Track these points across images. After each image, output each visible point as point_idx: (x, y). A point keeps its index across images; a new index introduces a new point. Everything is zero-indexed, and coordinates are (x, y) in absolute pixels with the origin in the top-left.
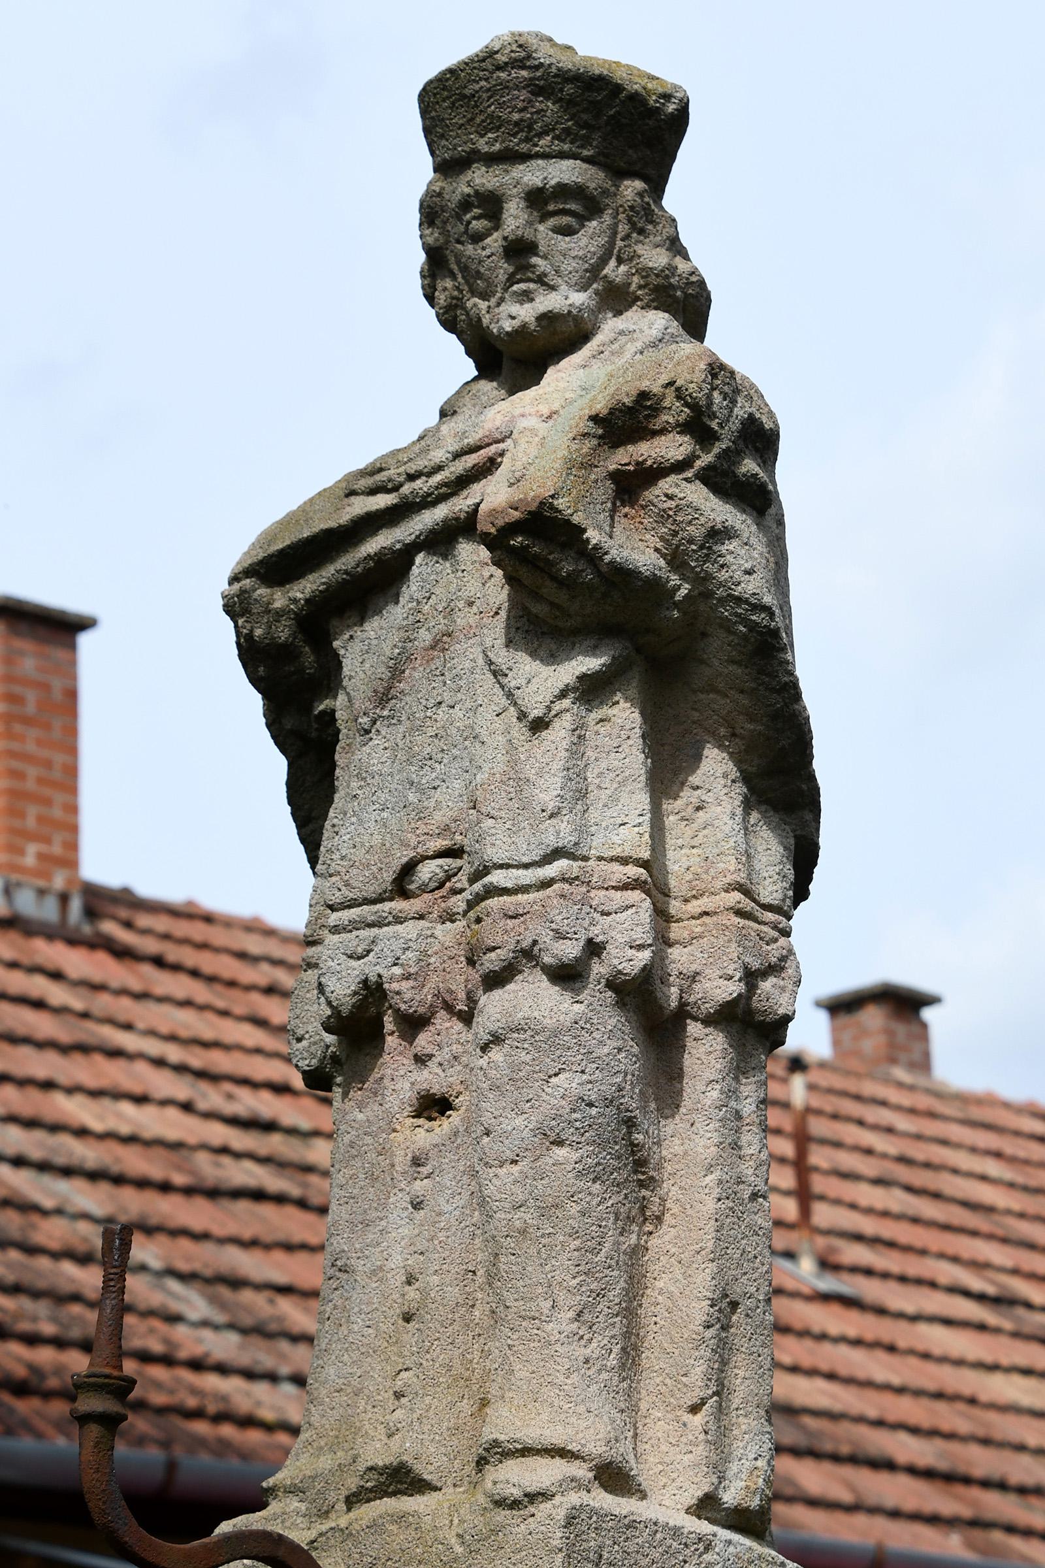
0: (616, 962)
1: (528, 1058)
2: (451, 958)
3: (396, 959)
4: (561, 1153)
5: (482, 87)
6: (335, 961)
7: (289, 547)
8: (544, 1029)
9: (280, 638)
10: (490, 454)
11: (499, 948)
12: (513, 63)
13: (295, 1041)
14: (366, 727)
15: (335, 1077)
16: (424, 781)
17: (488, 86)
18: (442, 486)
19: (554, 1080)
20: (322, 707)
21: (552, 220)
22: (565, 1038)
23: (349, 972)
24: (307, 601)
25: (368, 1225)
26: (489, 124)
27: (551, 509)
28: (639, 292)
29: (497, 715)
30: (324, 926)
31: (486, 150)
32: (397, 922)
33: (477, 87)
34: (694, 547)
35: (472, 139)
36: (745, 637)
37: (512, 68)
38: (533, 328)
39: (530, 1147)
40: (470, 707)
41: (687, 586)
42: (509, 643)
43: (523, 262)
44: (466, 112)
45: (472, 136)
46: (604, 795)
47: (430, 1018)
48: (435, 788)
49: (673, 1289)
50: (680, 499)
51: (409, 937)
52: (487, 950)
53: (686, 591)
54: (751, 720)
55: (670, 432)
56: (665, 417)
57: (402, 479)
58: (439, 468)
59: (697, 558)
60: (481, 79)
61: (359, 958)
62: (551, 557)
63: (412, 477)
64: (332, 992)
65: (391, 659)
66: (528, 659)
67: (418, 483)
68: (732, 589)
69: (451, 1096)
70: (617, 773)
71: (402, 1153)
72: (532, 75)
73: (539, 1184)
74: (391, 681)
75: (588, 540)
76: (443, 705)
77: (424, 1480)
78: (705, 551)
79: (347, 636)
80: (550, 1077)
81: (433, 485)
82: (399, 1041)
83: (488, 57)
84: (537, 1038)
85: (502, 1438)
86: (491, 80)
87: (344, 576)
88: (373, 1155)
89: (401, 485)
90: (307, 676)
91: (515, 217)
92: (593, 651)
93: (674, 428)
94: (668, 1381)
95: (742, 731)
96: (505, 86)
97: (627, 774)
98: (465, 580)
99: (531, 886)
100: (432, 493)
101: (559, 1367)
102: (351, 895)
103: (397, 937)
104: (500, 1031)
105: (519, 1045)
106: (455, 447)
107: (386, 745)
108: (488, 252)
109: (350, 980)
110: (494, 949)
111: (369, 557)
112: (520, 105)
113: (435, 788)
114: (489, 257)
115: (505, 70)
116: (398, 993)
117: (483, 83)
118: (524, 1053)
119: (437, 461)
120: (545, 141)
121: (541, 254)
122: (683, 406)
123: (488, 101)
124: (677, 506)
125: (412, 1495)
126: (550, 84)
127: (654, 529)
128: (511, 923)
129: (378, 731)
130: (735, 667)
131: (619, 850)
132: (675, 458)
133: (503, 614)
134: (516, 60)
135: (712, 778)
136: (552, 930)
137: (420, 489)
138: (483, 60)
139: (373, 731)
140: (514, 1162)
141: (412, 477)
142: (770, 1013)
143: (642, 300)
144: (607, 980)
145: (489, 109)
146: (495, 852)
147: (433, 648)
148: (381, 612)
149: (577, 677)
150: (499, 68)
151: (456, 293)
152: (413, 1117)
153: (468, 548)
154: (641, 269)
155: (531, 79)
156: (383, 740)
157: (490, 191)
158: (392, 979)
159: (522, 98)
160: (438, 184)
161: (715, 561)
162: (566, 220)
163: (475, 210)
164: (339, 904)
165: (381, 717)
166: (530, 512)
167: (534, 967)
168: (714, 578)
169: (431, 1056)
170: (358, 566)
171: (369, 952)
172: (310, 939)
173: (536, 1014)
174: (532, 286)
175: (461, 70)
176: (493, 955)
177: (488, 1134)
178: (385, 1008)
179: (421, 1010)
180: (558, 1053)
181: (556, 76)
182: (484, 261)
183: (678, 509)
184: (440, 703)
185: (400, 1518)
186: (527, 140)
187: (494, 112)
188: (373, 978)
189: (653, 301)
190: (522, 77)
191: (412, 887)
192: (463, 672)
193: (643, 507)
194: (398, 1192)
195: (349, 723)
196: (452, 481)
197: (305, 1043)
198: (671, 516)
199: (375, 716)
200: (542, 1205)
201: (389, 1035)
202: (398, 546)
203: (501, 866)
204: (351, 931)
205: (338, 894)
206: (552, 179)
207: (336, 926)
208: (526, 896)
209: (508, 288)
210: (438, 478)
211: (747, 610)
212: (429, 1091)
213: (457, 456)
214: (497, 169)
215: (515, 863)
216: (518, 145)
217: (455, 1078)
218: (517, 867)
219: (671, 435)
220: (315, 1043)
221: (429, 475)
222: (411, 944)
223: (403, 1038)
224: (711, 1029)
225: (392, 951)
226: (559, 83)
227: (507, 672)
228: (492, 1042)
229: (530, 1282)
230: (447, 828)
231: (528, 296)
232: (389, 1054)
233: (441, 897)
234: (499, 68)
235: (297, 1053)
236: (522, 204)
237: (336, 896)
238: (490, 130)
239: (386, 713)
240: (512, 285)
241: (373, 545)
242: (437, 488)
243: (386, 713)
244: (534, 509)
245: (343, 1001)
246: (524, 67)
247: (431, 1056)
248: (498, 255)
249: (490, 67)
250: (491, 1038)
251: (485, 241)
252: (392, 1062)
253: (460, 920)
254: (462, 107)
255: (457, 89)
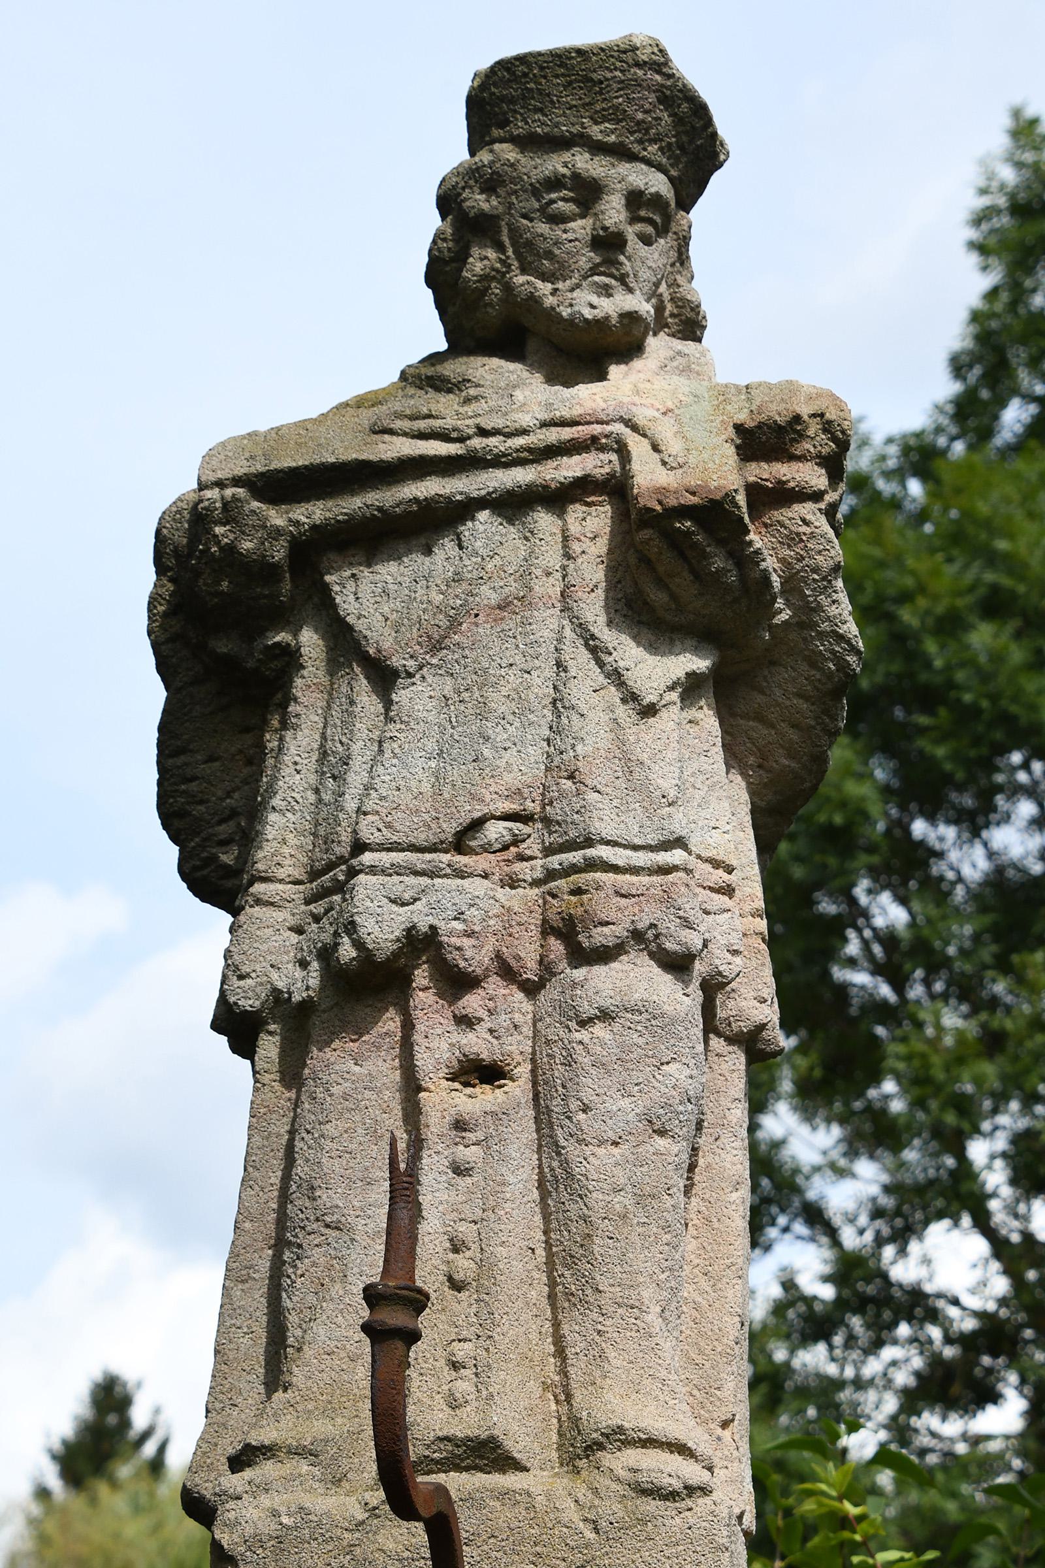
0: (717, 962)
1: (641, 1041)
2: (519, 924)
3: (459, 914)
4: (661, 1143)
5: (615, 77)
6: (375, 902)
7: (306, 467)
8: (663, 1015)
9: (273, 558)
10: (595, 433)
11: (613, 924)
12: (651, 64)
13: (235, 978)
14: (411, 670)
15: (268, 1024)
16: (498, 740)
17: (623, 78)
18: (525, 450)
19: (664, 1067)
20: (278, 639)
21: (639, 225)
22: (679, 1028)
23: (392, 916)
24: (314, 527)
25: (369, 1183)
26: (610, 114)
27: (732, 503)
28: (669, 320)
29: (594, 691)
30: (279, 864)
31: (600, 138)
32: (458, 876)
33: (609, 75)
34: (816, 577)
35: (584, 123)
36: (830, 675)
37: (650, 69)
38: (614, 323)
39: (634, 1131)
41: (788, 612)
42: (610, 623)
43: (612, 257)
44: (585, 95)
45: (584, 120)
46: (698, 795)
47: (481, 981)
48: (505, 749)
49: (700, 1300)
50: (816, 527)
51: (477, 893)
52: (599, 923)
53: (787, 617)
54: (791, 755)
55: (807, 460)
56: (807, 446)
57: (471, 431)
58: (524, 432)
59: (815, 588)
60: (616, 69)
61: (403, 905)
62: (708, 549)
63: (483, 432)
64: (369, 934)
65: (453, 608)
66: (633, 644)
67: (493, 441)
68: (837, 626)
69: (508, 1065)
70: (707, 776)
71: (439, 1115)
72: (664, 82)
73: (638, 1171)
74: (448, 630)
75: (751, 543)
76: (514, 667)
77: (513, 1458)
78: (825, 583)
79: (348, 573)
80: (662, 1064)
81: (513, 447)
82: (436, 998)
83: (630, 51)
84: (653, 1022)
85: (626, 1425)
86: (627, 73)
87: (376, 513)
88: (377, 1112)
89: (469, 438)
90: (277, 603)
91: (613, 211)
92: (696, 651)
93: (812, 458)
94: (695, 1392)
95: (774, 765)
96: (638, 84)
97: (715, 780)
98: (543, 549)
99: (643, 869)
100: (509, 455)
101: (660, 1362)
102: (395, 838)
103: (460, 892)
104: (612, 1008)
105: (632, 1026)
106: (545, 416)
107: (432, 693)
108: (570, 236)
109: (394, 925)
110: (607, 923)
111: (416, 500)
112: (647, 106)
113: (505, 749)
114: (570, 241)
115: (642, 69)
116: (459, 949)
117: (618, 73)
118: (635, 1036)
119: (525, 425)
120: (652, 148)
121: (627, 254)
122: (828, 439)
123: (617, 92)
124: (812, 533)
125: (489, 1473)
126: (673, 97)
127: (774, 549)
128: (624, 902)
129: (423, 677)
130: (801, 701)
131: (714, 852)
132: (819, 487)
133: (600, 593)
134: (655, 63)
135: (736, 803)
136: (680, 918)
137: (496, 447)
138: (625, 52)
139: (418, 676)
140: (615, 1144)
141: (483, 432)
142: (773, 1043)
143: (669, 328)
144: (704, 979)
145: (615, 100)
146: (605, 826)
147: (500, 607)
148: (400, 558)
149: (686, 674)
150: (638, 65)
151: (498, 265)
152: (448, 1079)
153: (546, 518)
154: (678, 298)
155: (662, 86)
156: (429, 688)
157: (594, 179)
158: (451, 934)
159: (650, 100)
160: (511, 154)
161: (830, 596)
162: (649, 230)
163: (566, 192)
164: (378, 844)
165: (429, 664)
166: (711, 500)
167: (641, 950)
168: (824, 611)
169: (480, 1020)
170: (398, 506)
171: (416, 900)
172: (263, 874)
173: (655, 998)
174: (613, 282)
175: (594, 54)
176: (606, 930)
177: (584, 1111)
178: (420, 962)
179: (479, 971)
180: (672, 1041)
181: (680, 91)
182: (564, 244)
183: (812, 536)
184: (511, 665)
185: (503, 1495)
186: (640, 142)
187: (620, 104)
188: (423, 927)
189: (679, 331)
190: (656, 81)
191: (473, 843)
192: (542, 640)
193: (766, 525)
194: (434, 1155)
195: (317, 662)
196: (539, 449)
197: (249, 981)
198: (803, 541)
199: (424, 661)
200: (639, 1192)
201: (420, 990)
202: (458, 497)
203: (608, 843)
204: (391, 875)
205: (377, 834)
206: (652, 186)
207: (372, 866)
208: (634, 879)
209: (588, 277)
210: (520, 441)
211: (845, 650)
212: (479, 1055)
213: (544, 424)
214: (606, 160)
215: (624, 842)
216: (632, 143)
217: (515, 1047)
218: (625, 847)
219: (809, 463)
220: (261, 984)
221: (509, 435)
222: (477, 901)
223: (440, 995)
224: (736, 1048)
225: (454, 904)
226: (680, 99)
227: (612, 651)
228: (598, 1018)
229: (629, 1269)
230: (519, 792)
231: (607, 290)
232: (422, 1010)
233: (504, 861)
234: (638, 65)
235: (239, 991)
236: (623, 202)
237: (375, 835)
238: (609, 121)
239: (434, 661)
240: (592, 275)
241: (430, 487)
242: (517, 451)
243: (434, 661)
244: (718, 498)
245: (383, 945)
246: (659, 72)
247: (480, 1020)
248: (583, 242)
249: (631, 61)
250: (598, 1014)
251: (569, 225)
252: (426, 1018)
253: (525, 888)
254: (581, 88)
255: (583, 70)
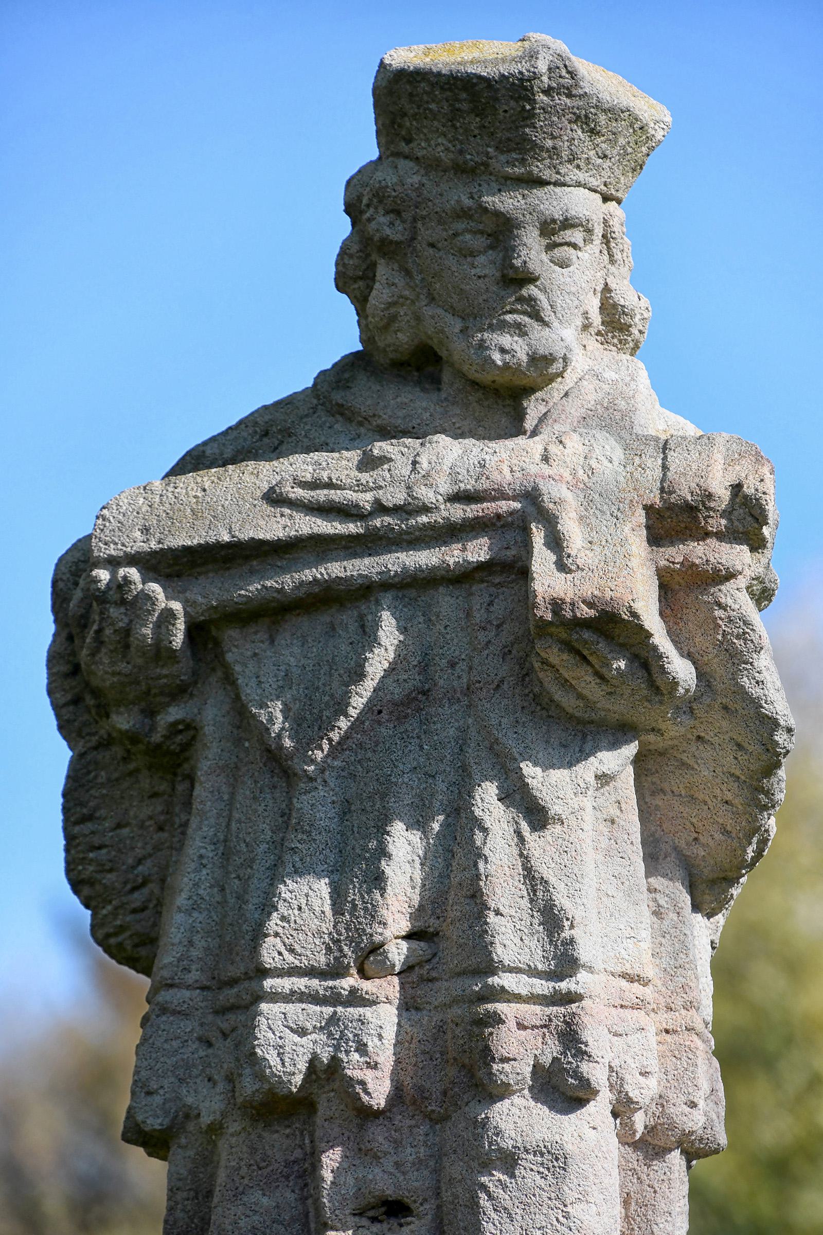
11: (515, 1060)
13: (143, 1095)
40: (454, 780)
69: (415, 1202)
107: (334, 798)
156: (331, 793)
173: (557, 1138)
231: (521, 330)
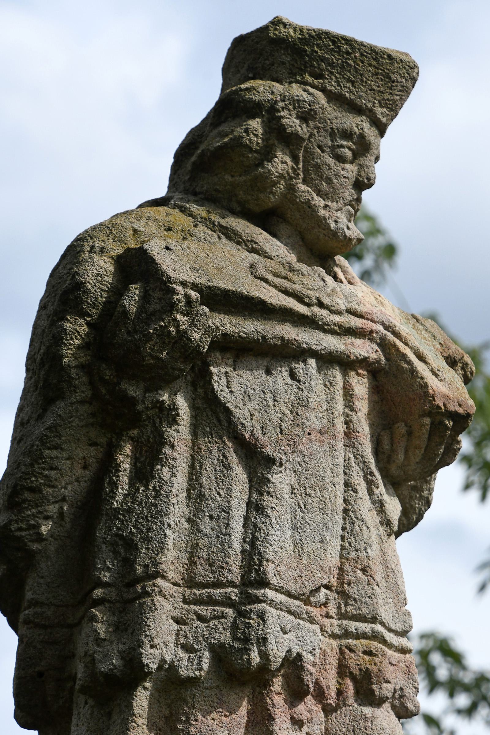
5: (402, 82)
31: (380, 117)
33: (399, 79)
60: (404, 77)
67: (324, 313)
114: (345, 177)
145: (395, 97)
178: (279, 674)
202: (305, 346)
204: (277, 609)
210: (336, 318)
215: (387, 625)
221: (332, 312)
253: (325, 637)
